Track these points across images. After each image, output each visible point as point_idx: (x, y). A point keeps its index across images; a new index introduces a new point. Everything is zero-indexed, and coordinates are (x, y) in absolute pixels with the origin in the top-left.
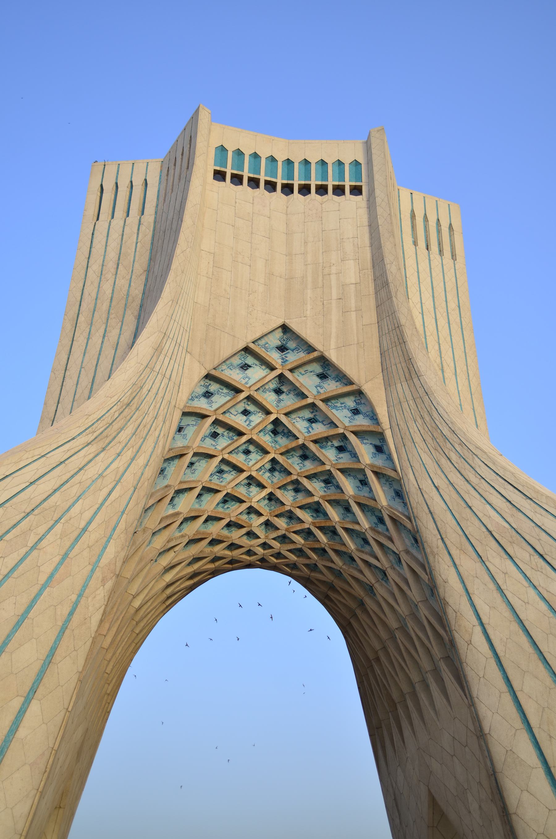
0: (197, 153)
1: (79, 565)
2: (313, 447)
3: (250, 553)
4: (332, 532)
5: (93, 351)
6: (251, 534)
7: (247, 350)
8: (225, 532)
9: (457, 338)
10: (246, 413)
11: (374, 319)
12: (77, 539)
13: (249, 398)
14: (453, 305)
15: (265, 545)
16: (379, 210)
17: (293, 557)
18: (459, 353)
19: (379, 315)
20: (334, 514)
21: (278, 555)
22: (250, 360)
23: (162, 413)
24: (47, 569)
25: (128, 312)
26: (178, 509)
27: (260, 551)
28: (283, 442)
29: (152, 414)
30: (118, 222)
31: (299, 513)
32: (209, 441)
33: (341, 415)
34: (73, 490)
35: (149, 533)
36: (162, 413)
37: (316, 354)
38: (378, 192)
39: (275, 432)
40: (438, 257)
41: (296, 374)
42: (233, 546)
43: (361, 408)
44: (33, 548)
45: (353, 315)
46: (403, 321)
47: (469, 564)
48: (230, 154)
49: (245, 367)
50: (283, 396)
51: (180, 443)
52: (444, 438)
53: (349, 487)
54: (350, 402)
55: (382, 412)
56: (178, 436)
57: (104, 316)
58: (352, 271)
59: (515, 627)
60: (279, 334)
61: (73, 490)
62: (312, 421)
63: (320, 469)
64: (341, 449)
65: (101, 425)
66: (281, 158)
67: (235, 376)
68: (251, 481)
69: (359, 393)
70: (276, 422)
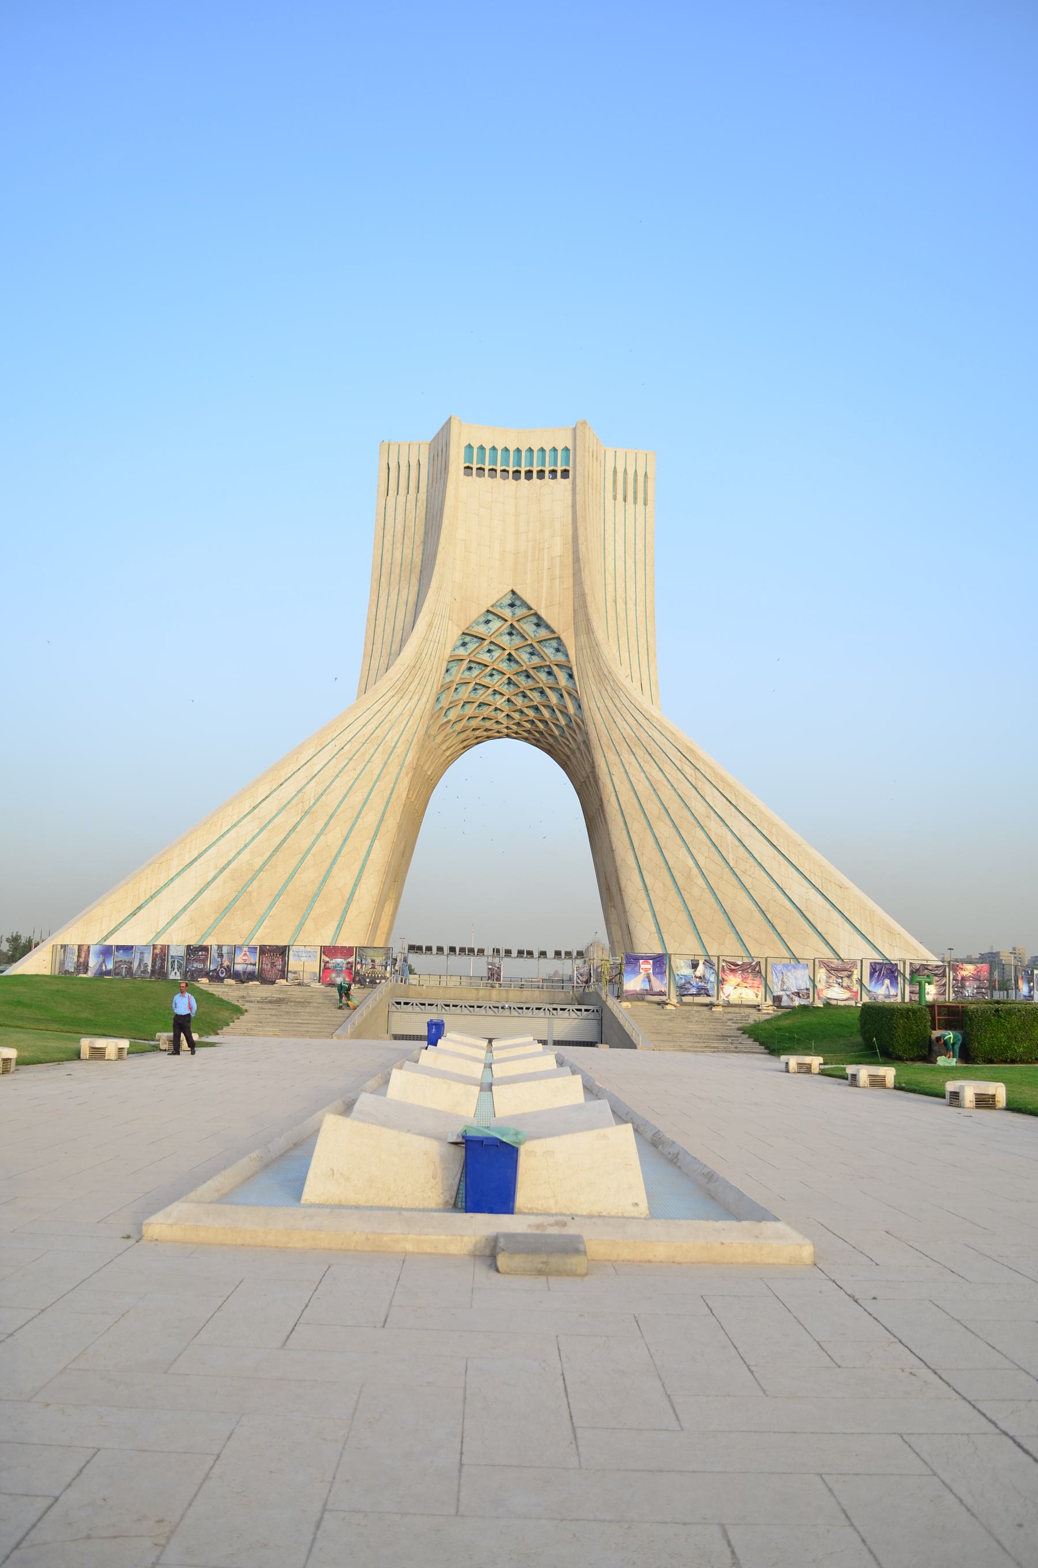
1: (393, 768)
2: (531, 672)
3: (498, 732)
4: (544, 722)
5: (392, 606)
6: (497, 722)
7: (488, 611)
8: (482, 723)
9: (640, 574)
10: (489, 651)
11: (571, 584)
12: (391, 754)
13: (491, 642)
14: (640, 546)
15: (507, 728)
16: (578, 497)
17: (526, 734)
20: (546, 714)
21: (516, 733)
22: (490, 617)
24: (376, 772)
25: (413, 576)
26: (450, 717)
27: (505, 731)
29: (429, 669)
31: (525, 710)
32: (467, 673)
33: (549, 651)
34: (387, 725)
37: (532, 612)
39: (509, 660)
41: (521, 623)
42: (487, 730)
43: (561, 648)
44: (369, 761)
45: (557, 582)
47: (612, 757)
48: (475, 450)
49: (488, 622)
52: (604, 676)
53: (553, 698)
54: (554, 644)
55: (572, 653)
56: (447, 675)
57: (398, 578)
58: (558, 547)
59: (632, 794)
61: (387, 725)
62: (532, 654)
63: (537, 686)
64: (550, 673)
65: (399, 683)
66: (512, 449)
67: (481, 630)
69: (558, 639)
70: (510, 654)
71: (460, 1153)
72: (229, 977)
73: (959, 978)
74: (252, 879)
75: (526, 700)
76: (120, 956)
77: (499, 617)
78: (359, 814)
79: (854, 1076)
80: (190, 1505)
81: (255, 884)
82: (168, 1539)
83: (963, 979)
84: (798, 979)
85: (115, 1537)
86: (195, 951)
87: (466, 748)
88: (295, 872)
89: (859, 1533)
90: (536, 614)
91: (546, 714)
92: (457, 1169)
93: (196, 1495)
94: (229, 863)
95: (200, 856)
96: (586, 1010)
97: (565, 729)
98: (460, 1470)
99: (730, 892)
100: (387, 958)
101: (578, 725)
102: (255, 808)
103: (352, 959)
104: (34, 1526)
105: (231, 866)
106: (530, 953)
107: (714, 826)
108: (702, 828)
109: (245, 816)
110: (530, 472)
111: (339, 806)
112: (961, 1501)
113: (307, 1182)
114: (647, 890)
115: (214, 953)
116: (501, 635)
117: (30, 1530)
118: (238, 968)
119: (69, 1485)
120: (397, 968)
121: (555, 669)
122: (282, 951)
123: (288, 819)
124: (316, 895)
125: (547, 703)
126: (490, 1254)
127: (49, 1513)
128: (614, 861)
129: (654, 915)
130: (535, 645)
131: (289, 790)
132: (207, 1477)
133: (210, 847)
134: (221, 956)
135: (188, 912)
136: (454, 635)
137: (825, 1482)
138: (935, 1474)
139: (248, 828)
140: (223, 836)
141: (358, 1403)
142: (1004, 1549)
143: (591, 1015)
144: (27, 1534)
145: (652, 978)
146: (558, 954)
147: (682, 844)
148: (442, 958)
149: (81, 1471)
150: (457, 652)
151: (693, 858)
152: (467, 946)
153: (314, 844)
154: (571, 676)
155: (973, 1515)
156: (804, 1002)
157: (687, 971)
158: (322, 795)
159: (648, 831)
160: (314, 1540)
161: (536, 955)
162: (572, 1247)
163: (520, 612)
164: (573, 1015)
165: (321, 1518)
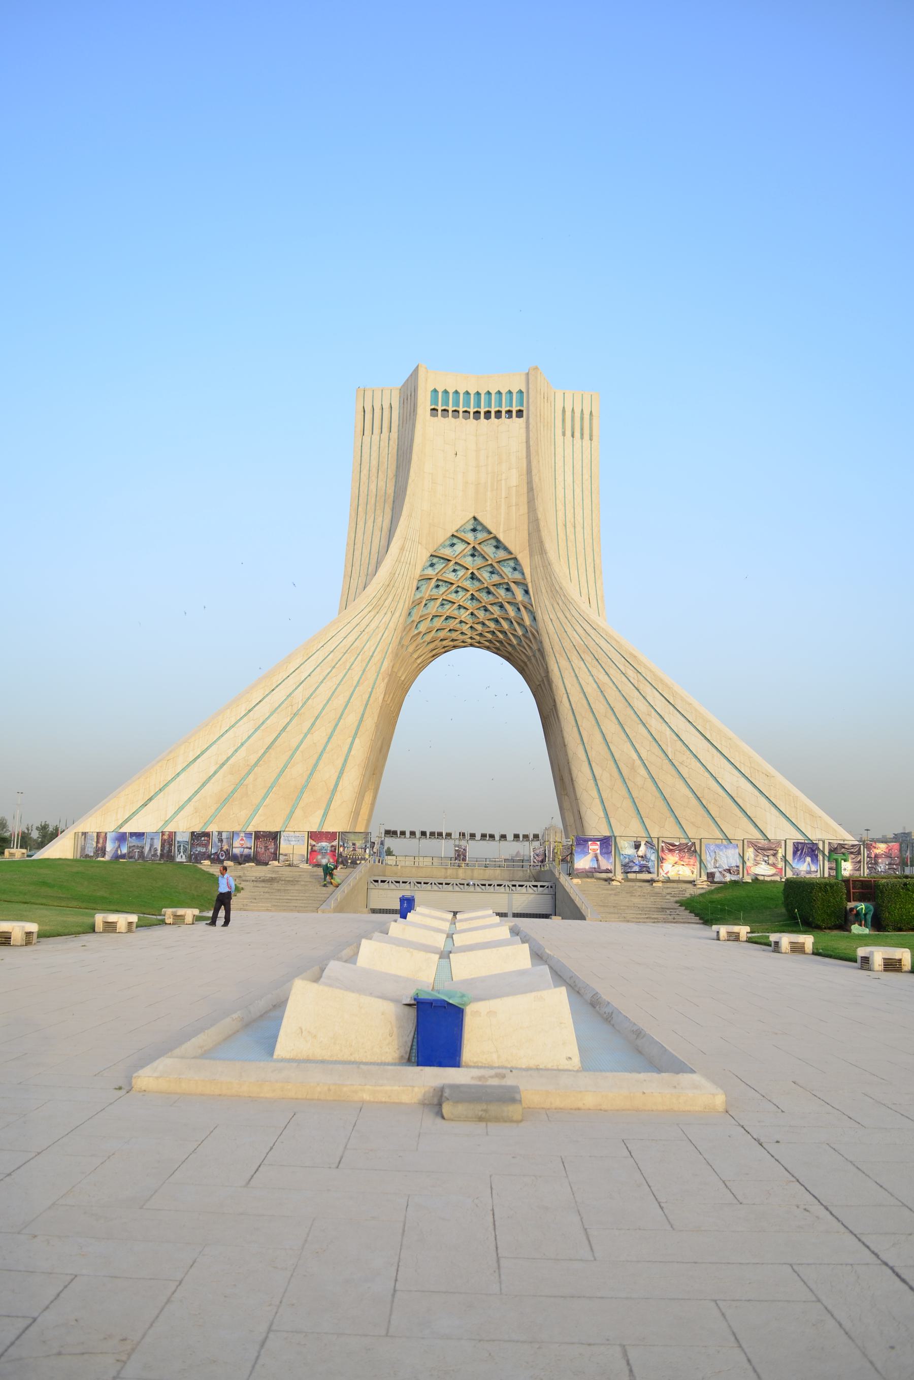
0: (419, 404)
1: (371, 675)
2: (492, 589)
4: (504, 632)
5: (369, 532)
7: (453, 535)
8: (449, 634)
9: (587, 501)
10: (454, 571)
11: (526, 511)
14: (586, 476)
15: (471, 638)
16: (531, 434)
17: (487, 644)
18: (587, 512)
19: (529, 508)
20: (505, 625)
21: (479, 643)
22: (455, 541)
23: (406, 585)
24: (356, 679)
25: (387, 506)
26: (420, 630)
27: (469, 641)
28: (476, 583)
30: (376, 437)
31: (487, 622)
32: (435, 590)
33: (507, 570)
34: (365, 637)
35: (405, 648)
36: (406, 585)
37: (492, 536)
38: (531, 420)
39: (472, 578)
40: (580, 441)
41: (482, 546)
42: (453, 640)
43: (517, 567)
46: (540, 516)
47: (563, 663)
49: (453, 545)
50: (476, 558)
51: (418, 597)
52: (556, 591)
53: (512, 612)
54: (512, 563)
56: (417, 592)
57: (373, 507)
58: (514, 478)
59: (582, 695)
60: (472, 521)
62: (492, 573)
63: (496, 601)
64: (508, 590)
65: (375, 600)
66: (472, 392)
67: (447, 552)
68: (460, 607)
69: (515, 559)
70: (472, 573)
71: (413, 1012)
72: (228, 860)
73: (873, 856)
74: (249, 773)
75: (487, 613)
76: (133, 841)
77: (463, 540)
78: (342, 715)
79: (777, 943)
80: (151, 1325)
81: (251, 777)
82: (129, 1355)
83: (876, 856)
84: (729, 858)
85: (83, 1354)
86: (199, 837)
87: (435, 656)
88: (285, 766)
89: (745, 1354)
90: (495, 538)
91: (505, 625)
92: (411, 1027)
93: (157, 1317)
94: (228, 759)
95: (202, 753)
96: (541, 886)
97: (522, 638)
98: (393, 1295)
99: (668, 780)
100: (366, 842)
101: (533, 634)
102: (250, 711)
103: (335, 843)
104: (12, 1344)
105: (230, 762)
106: (492, 836)
107: (654, 723)
108: (644, 725)
109: (241, 718)
110: (489, 412)
111: (323, 708)
112: (840, 1325)
113: (279, 1039)
114: (595, 780)
115: (215, 838)
116: (465, 556)
117: (9, 1347)
118: (237, 851)
119: (47, 1307)
120: (375, 850)
121: (513, 586)
122: (274, 837)
123: (280, 720)
124: (305, 787)
125: (506, 616)
126: (436, 1103)
127: (27, 1332)
128: (566, 754)
129: (602, 802)
130: (495, 565)
131: (280, 695)
132: (168, 1301)
133: (210, 746)
134: (221, 841)
135: (192, 803)
136: (423, 557)
137: (719, 1308)
138: (819, 1301)
139: (244, 728)
140: (222, 736)
141: (308, 1235)
142: (876, 1369)
143: (546, 891)
144: (6, 1350)
145: (600, 857)
146: (516, 836)
147: (626, 739)
148: (414, 841)
149: (58, 1295)
150: (426, 572)
151: (636, 751)
152: (436, 830)
153: (302, 742)
154: (527, 592)
155: (850, 1337)
156: (734, 878)
157: (630, 851)
158: (308, 699)
159: (596, 727)
160: (257, 1358)
161: (497, 838)
162: (509, 1096)
163: (481, 536)
164: (530, 891)
165: (266, 1338)
